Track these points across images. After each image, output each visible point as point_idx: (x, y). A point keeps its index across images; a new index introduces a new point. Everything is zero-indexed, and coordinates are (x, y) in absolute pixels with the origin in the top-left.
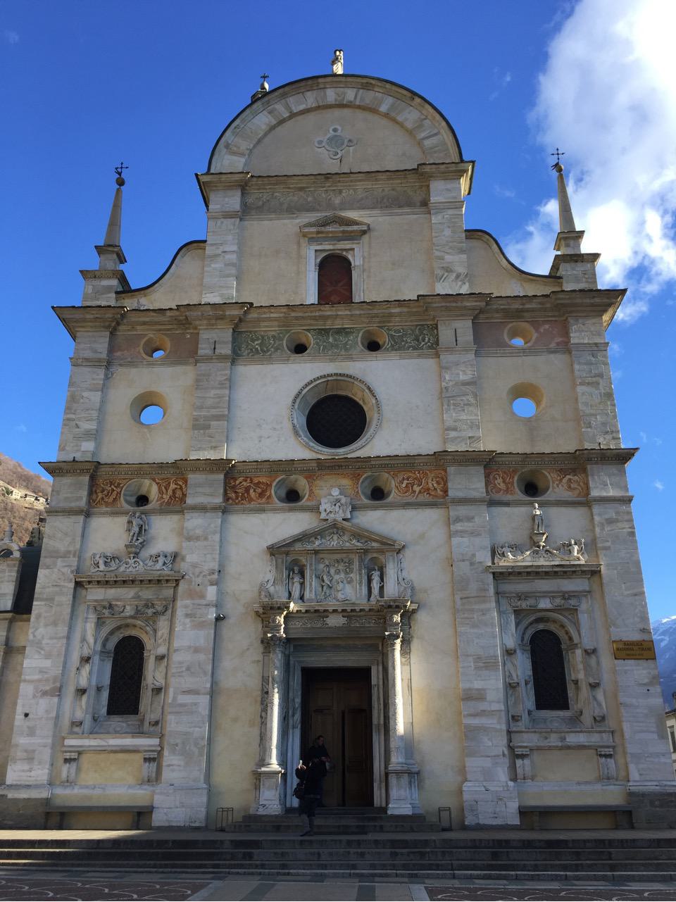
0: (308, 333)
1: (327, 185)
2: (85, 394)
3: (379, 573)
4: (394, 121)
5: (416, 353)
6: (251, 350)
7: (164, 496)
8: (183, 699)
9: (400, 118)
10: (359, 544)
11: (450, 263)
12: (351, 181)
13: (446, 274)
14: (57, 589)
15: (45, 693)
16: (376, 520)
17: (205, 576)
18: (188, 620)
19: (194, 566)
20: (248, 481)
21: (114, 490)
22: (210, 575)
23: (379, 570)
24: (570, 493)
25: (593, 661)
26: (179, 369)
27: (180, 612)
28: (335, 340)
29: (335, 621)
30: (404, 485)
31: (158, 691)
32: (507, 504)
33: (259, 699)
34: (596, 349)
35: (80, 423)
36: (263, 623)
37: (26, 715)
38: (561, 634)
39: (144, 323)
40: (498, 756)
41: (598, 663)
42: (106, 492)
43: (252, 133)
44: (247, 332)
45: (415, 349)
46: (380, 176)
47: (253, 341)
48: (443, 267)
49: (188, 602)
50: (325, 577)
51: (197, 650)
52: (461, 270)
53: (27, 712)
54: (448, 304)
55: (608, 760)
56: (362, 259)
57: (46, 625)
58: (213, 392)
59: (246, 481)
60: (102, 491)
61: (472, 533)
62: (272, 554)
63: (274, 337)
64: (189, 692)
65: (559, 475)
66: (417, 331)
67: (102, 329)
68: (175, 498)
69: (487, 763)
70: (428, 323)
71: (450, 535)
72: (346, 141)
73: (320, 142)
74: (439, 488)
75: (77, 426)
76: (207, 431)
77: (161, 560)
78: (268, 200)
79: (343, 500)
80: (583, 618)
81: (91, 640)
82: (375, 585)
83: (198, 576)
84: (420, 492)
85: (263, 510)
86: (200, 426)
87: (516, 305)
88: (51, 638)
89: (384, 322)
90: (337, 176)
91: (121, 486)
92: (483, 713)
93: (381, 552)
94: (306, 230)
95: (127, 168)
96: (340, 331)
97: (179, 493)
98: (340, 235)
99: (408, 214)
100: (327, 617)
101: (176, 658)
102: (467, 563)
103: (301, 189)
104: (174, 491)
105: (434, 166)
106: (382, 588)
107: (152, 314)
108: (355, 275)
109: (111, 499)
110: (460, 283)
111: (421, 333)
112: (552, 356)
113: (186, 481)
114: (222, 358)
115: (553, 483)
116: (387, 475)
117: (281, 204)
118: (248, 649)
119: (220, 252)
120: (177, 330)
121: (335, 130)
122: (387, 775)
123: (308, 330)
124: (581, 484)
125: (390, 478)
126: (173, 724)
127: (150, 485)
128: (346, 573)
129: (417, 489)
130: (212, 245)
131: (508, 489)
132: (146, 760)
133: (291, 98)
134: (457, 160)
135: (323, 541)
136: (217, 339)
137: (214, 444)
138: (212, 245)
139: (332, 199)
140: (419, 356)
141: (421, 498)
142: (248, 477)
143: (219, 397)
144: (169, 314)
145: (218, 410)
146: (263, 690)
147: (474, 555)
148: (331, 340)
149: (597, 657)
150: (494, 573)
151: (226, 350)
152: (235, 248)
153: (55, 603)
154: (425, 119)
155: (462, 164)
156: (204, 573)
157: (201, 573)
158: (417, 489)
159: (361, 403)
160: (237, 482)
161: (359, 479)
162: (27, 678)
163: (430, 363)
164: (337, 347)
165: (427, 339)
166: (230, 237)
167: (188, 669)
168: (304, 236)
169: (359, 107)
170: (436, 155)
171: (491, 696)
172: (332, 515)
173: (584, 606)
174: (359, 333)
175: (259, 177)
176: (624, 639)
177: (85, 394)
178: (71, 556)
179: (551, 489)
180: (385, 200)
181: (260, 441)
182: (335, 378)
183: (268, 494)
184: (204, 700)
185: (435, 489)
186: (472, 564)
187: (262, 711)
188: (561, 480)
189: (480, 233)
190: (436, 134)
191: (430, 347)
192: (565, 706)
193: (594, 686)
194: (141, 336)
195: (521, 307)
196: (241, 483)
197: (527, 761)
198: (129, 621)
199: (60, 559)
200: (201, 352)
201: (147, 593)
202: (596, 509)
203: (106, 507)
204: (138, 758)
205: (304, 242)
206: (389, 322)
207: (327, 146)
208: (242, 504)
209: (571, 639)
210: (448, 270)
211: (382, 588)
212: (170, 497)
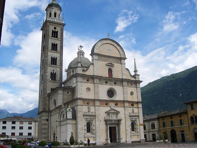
8: (98, 131)
15: (81, 130)
16: (117, 109)
19: (97, 114)
29: (113, 121)
32: (130, 107)
51: (99, 125)
64: (98, 130)
69: (129, 137)
82: (117, 117)
85: (104, 106)
92: (128, 132)
94: (107, 64)
112: (135, 88)
113: (95, 102)
122: (118, 139)
130: (95, 64)
138: (95, 64)
141: (122, 106)
166: (97, 64)
167: (98, 127)
169: (112, 45)
171: (129, 130)
201: (91, 117)
202: (139, 108)
204: (93, 137)
205: (106, 66)
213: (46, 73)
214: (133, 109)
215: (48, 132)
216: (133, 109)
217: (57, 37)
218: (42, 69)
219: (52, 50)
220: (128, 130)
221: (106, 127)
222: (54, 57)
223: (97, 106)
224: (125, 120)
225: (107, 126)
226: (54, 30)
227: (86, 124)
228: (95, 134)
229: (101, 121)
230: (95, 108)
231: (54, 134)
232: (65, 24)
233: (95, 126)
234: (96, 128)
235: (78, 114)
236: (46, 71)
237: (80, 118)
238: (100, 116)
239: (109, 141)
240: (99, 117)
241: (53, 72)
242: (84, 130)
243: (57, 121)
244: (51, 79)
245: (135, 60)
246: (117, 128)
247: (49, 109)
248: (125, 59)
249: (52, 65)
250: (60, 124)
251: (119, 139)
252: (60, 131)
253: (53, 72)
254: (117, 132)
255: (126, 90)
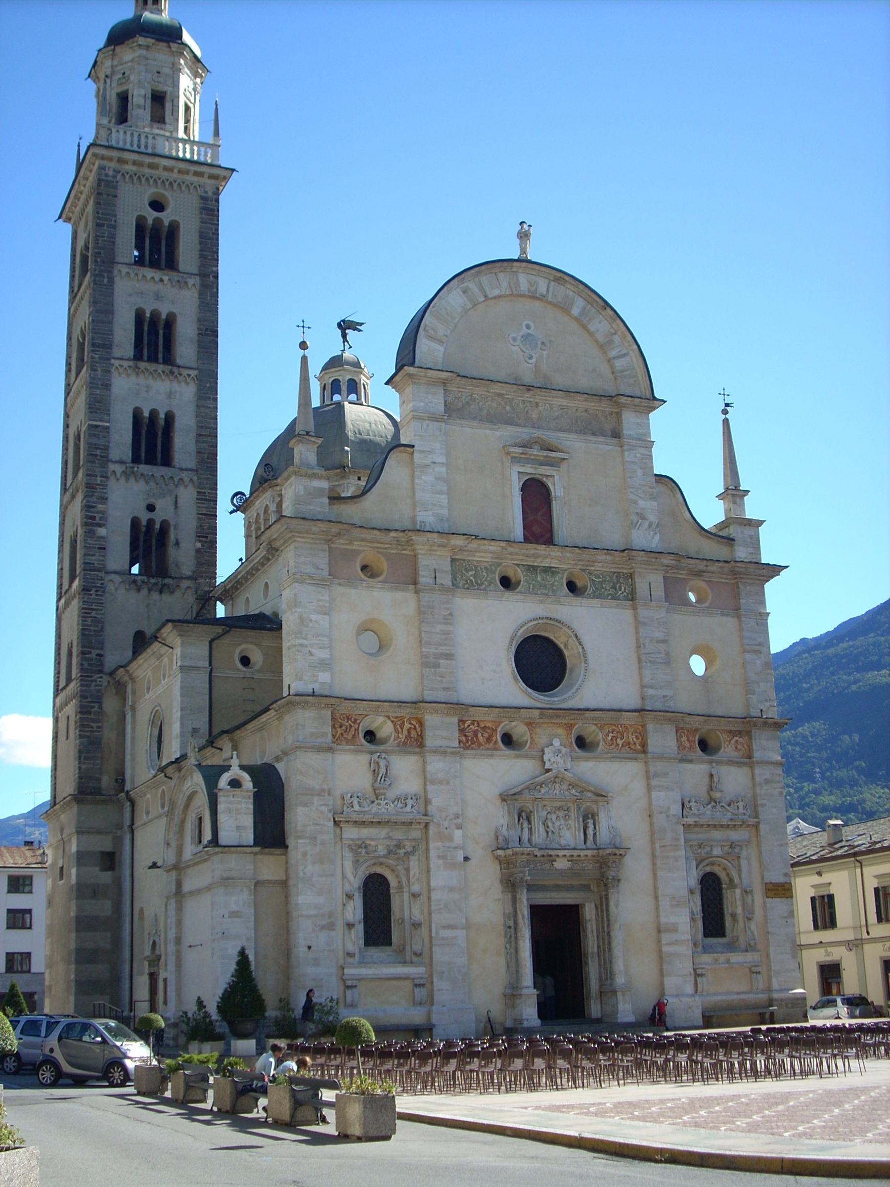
0: (519, 570)
1: (526, 395)
2: (313, 617)
3: (592, 821)
4: (584, 327)
5: (614, 602)
6: (466, 581)
7: (400, 736)
9: (592, 328)
10: (577, 794)
11: (643, 509)
12: (550, 397)
13: (640, 521)
14: (318, 827)
15: (323, 928)
17: (450, 820)
18: (441, 862)
19: (440, 809)
20: (476, 725)
21: (351, 726)
22: (455, 819)
23: (592, 818)
24: (736, 754)
25: (749, 899)
26: (399, 595)
27: (433, 854)
28: (543, 579)
29: (561, 864)
30: (610, 738)
31: (417, 925)
33: (503, 933)
34: (759, 618)
35: (312, 650)
36: (500, 865)
37: (309, 948)
38: (723, 876)
39: (363, 540)
40: (687, 975)
41: (753, 900)
42: (344, 728)
43: (448, 314)
44: (461, 560)
45: (613, 598)
46: (578, 396)
47: (467, 570)
48: (637, 513)
49: (439, 844)
50: (550, 824)
51: (451, 889)
52: (652, 518)
53: (310, 945)
54: (649, 559)
55: (758, 975)
56: (562, 489)
57: (314, 863)
58: (438, 628)
59: (474, 724)
60: (341, 727)
61: (667, 788)
62: (504, 800)
63: (486, 568)
65: (728, 736)
66: (614, 577)
67: (322, 542)
68: (411, 738)
70: (625, 571)
71: (649, 788)
72: (539, 343)
73: (514, 339)
74: (638, 742)
75: (311, 654)
76: (437, 670)
77: (410, 802)
78: (468, 403)
79: (564, 750)
80: (744, 863)
81: (351, 877)
82: (590, 831)
83: (445, 820)
84: (623, 745)
86: (429, 663)
87: (701, 566)
88: (321, 876)
89: (587, 566)
90: (539, 390)
91: (358, 721)
92: (676, 942)
93: (596, 802)
95: (303, 321)
96: (547, 570)
97: (413, 734)
98: (542, 458)
99: (601, 443)
100: (555, 861)
101: (434, 896)
102: (664, 815)
103: (500, 395)
104: (409, 730)
105: (630, 399)
106: (595, 834)
107: (376, 532)
108: (555, 506)
109: (350, 737)
110: (652, 533)
111: (618, 581)
112: (724, 618)
113: (421, 724)
114: (445, 590)
115: (725, 742)
116: (594, 727)
117: (481, 409)
118: (490, 888)
119: (428, 462)
120: (393, 549)
121: (528, 327)
123: (518, 565)
124: (745, 746)
125: (598, 730)
126: (440, 955)
127: (385, 722)
128: (566, 820)
129: (620, 742)
131: (691, 746)
132: (416, 985)
133: (484, 278)
134: (649, 395)
135: (547, 789)
136: (437, 567)
137: (445, 685)
138: (421, 452)
139: (530, 412)
140: (617, 606)
142: (474, 721)
143: (444, 634)
144: (393, 534)
145: (444, 648)
146: (505, 925)
147: (669, 808)
148: (539, 579)
149: (753, 896)
150: (683, 825)
151: (446, 580)
152: (442, 459)
153: (319, 842)
154: (615, 334)
155: (655, 402)
156: (449, 818)
157: (447, 816)
158: (620, 742)
159: (562, 646)
160: (466, 725)
161: (572, 730)
162: (305, 913)
163: (627, 614)
164: (545, 586)
165: (623, 588)
166: (437, 445)
167: (446, 906)
168: (508, 453)
170: (626, 380)
172: (555, 765)
173: (744, 854)
174: (564, 574)
175: (464, 377)
176: (773, 881)
177: (313, 617)
178: (326, 794)
179: (723, 749)
180: (579, 423)
181: (483, 683)
182: (545, 621)
183: (494, 738)
184: (461, 934)
185: (635, 744)
186: (668, 817)
187: (507, 943)
188: (730, 741)
189: (666, 479)
190: (625, 355)
191: (626, 598)
192: (723, 935)
193: (749, 919)
194: (358, 552)
195: (704, 568)
196: (469, 726)
197: (704, 979)
198: (381, 860)
199: (316, 798)
200: (422, 580)
201: (398, 834)
202: (757, 771)
203: (347, 744)
206: (592, 566)
207: (521, 345)
208: (473, 749)
209: (731, 880)
210: (643, 518)
211: (595, 834)
212: (406, 737)
213: (100, 525)
214: (711, 776)
215: (117, 943)
216: (711, 776)
217: (171, 264)
218: (73, 497)
219: (138, 357)
220: (673, 929)
221: (509, 909)
222: (154, 413)
223: (436, 751)
224: (654, 857)
225: (514, 900)
226: (151, 215)
227: (355, 882)
228: (427, 961)
229: (466, 859)
230: (425, 763)
231: (155, 961)
232: (233, 170)
233: (424, 898)
234: (430, 914)
235: (301, 810)
236: (100, 507)
237: (313, 838)
238: (459, 827)
239: (529, 1013)
240: (458, 833)
241: (144, 517)
242: (340, 925)
243: (154, 866)
244: (135, 570)
245: (725, 412)
246: (589, 913)
247: (123, 780)
248: (651, 401)
249: (143, 468)
250: (179, 884)
251: (608, 991)
252: (178, 940)
253: (150, 515)
254: (591, 944)
255: (659, 635)
